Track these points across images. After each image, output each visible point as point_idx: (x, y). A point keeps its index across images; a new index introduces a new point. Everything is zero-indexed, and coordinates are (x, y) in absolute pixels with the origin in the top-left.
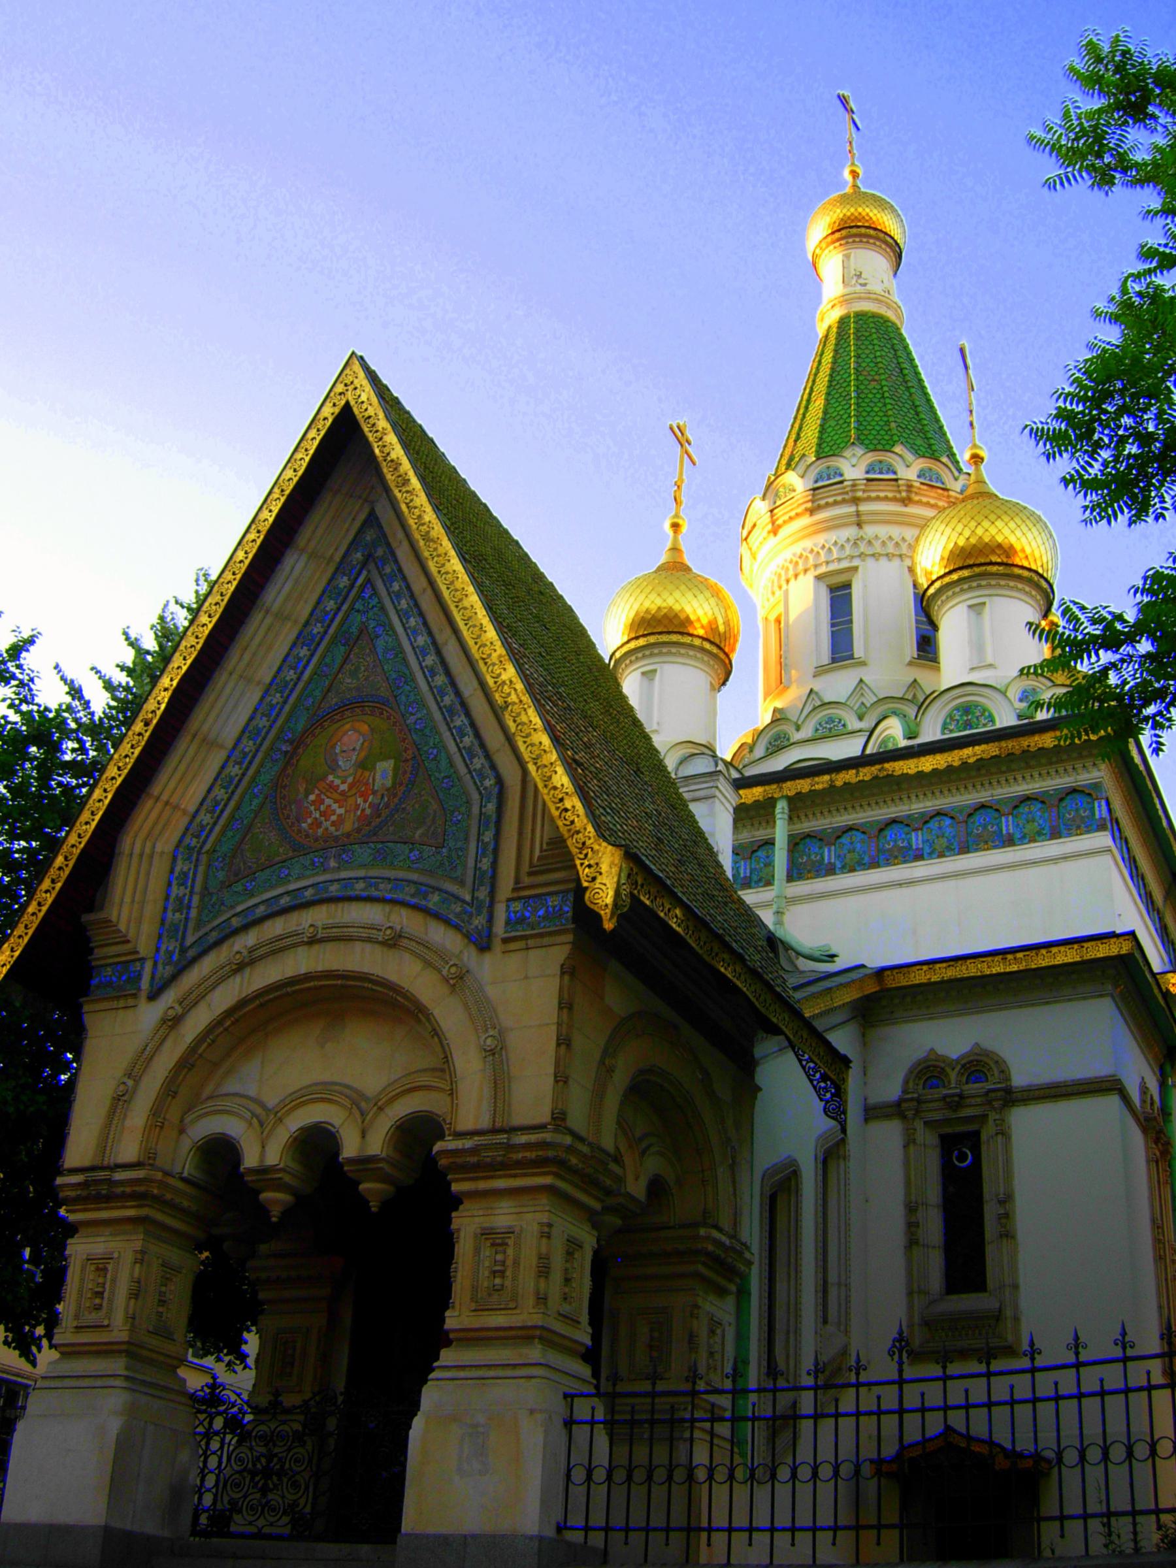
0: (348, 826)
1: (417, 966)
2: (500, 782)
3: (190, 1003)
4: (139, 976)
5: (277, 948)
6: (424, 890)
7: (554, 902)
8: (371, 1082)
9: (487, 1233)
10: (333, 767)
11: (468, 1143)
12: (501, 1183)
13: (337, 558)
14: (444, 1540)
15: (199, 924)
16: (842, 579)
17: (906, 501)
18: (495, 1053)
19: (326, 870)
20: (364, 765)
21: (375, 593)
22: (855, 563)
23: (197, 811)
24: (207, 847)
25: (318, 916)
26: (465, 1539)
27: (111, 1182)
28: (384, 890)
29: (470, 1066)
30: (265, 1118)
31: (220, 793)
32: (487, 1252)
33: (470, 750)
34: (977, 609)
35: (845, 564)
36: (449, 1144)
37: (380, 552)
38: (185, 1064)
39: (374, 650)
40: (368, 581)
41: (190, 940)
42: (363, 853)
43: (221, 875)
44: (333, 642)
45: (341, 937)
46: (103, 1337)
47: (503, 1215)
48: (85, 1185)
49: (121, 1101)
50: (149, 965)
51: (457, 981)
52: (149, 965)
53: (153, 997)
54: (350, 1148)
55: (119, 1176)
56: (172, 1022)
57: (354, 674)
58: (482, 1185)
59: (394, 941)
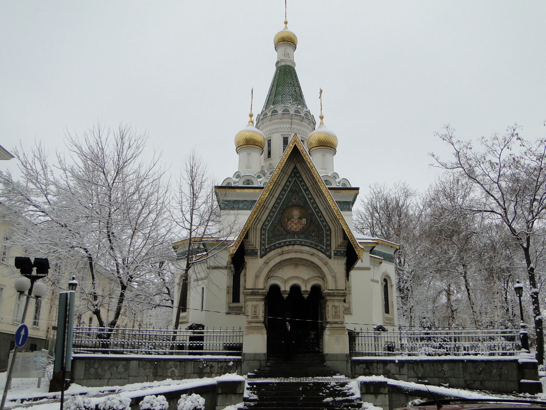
0: (298, 230)
1: (317, 260)
2: (330, 228)
3: (270, 260)
4: (257, 252)
5: (288, 252)
6: (316, 246)
7: (342, 252)
8: (306, 278)
9: (334, 306)
10: (293, 218)
11: (331, 292)
12: (336, 298)
13: (289, 174)
14: (334, 355)
15: (268, 244)
16: (286, 136)
17: (302, 121)
18: (334, 277)
19: (295, 238)
20: (300, 218)
21: (297, 183)
22: (290, 133)
23: (265, 222)
24: (268, 228)
25: (296, 247)
26: (337, 355)
27: (258, 292)
28: (308, 244)
29: (329, 277)
30: (285, 282)
31: (269, 219)
32: (334, 309)
33: (323, 221)
34: (324, 156)
35: (287, 133)
36: (326, 291)
37: (298, 175)
38: (270, 271)
39: (298, 195)
40: (295, 180)
41: (267, 247)
42: (303, 236)
43: (271, 235)
44: (289, 192)
45: (301, 252)
46: (258, 320)
47: (336, 304)
48: (252, 292)
49: (257, 277)
50: (259, 251)
51: (326, 264)
52: (259, 251)
53: (261, 257)
54: (303, 288)
55: (260, 291)
56: (266, 263)
57: (295, 199)
58: (332, 298)
59: (313, 255)
